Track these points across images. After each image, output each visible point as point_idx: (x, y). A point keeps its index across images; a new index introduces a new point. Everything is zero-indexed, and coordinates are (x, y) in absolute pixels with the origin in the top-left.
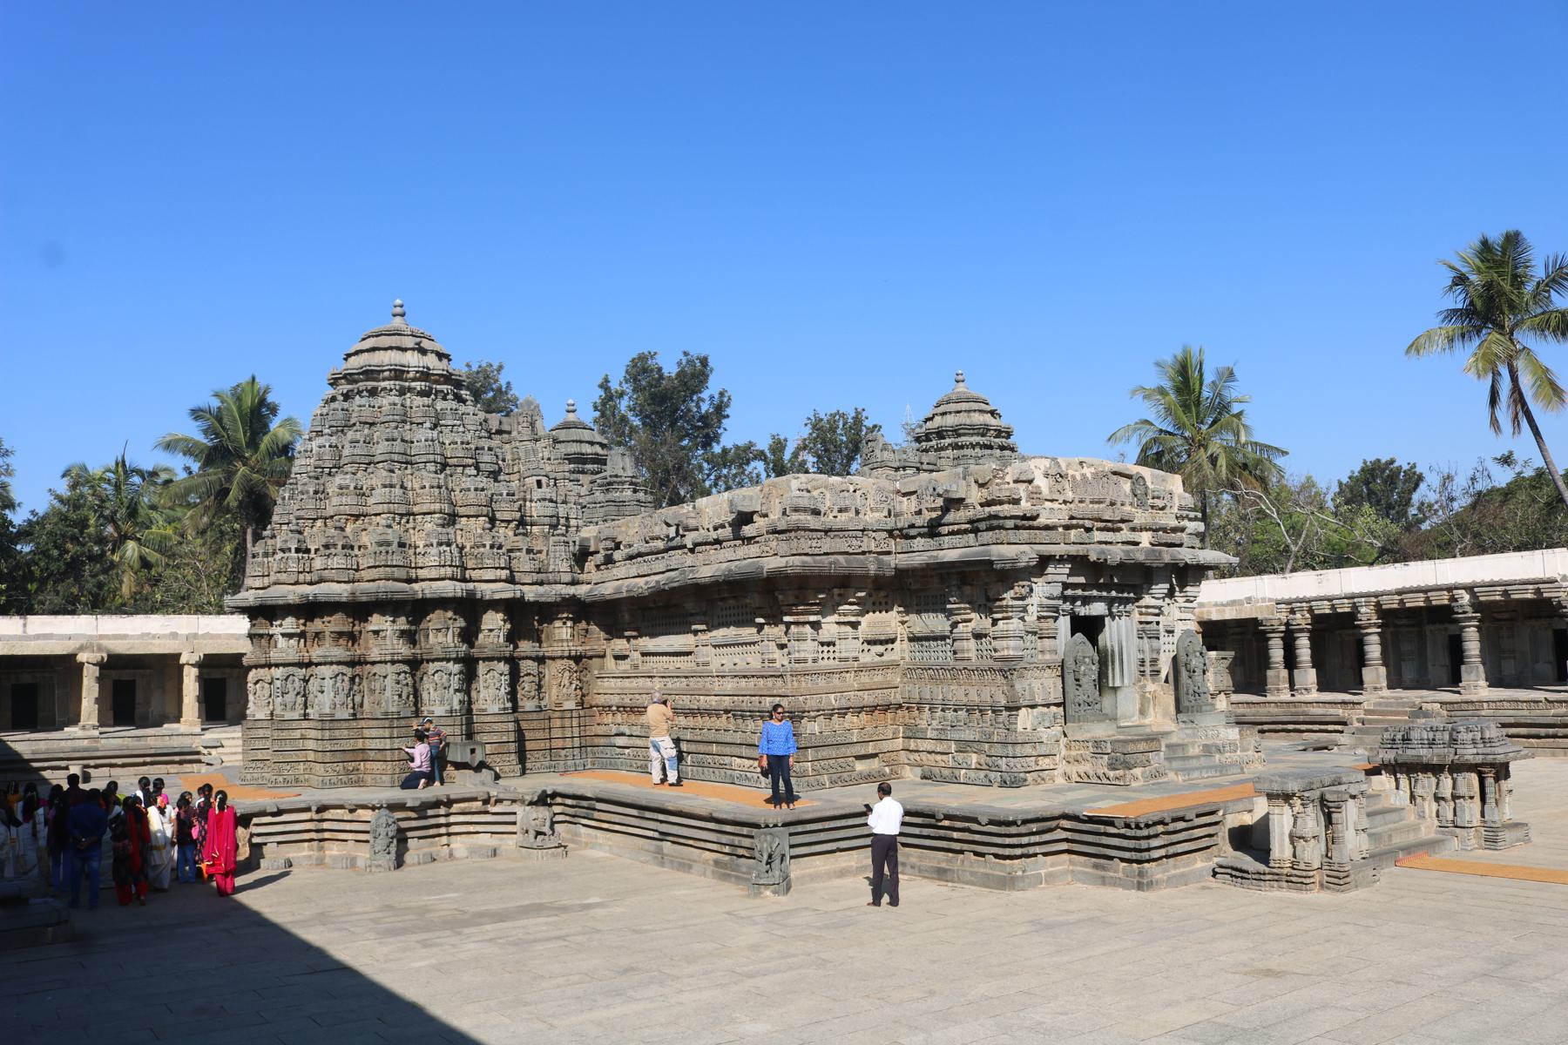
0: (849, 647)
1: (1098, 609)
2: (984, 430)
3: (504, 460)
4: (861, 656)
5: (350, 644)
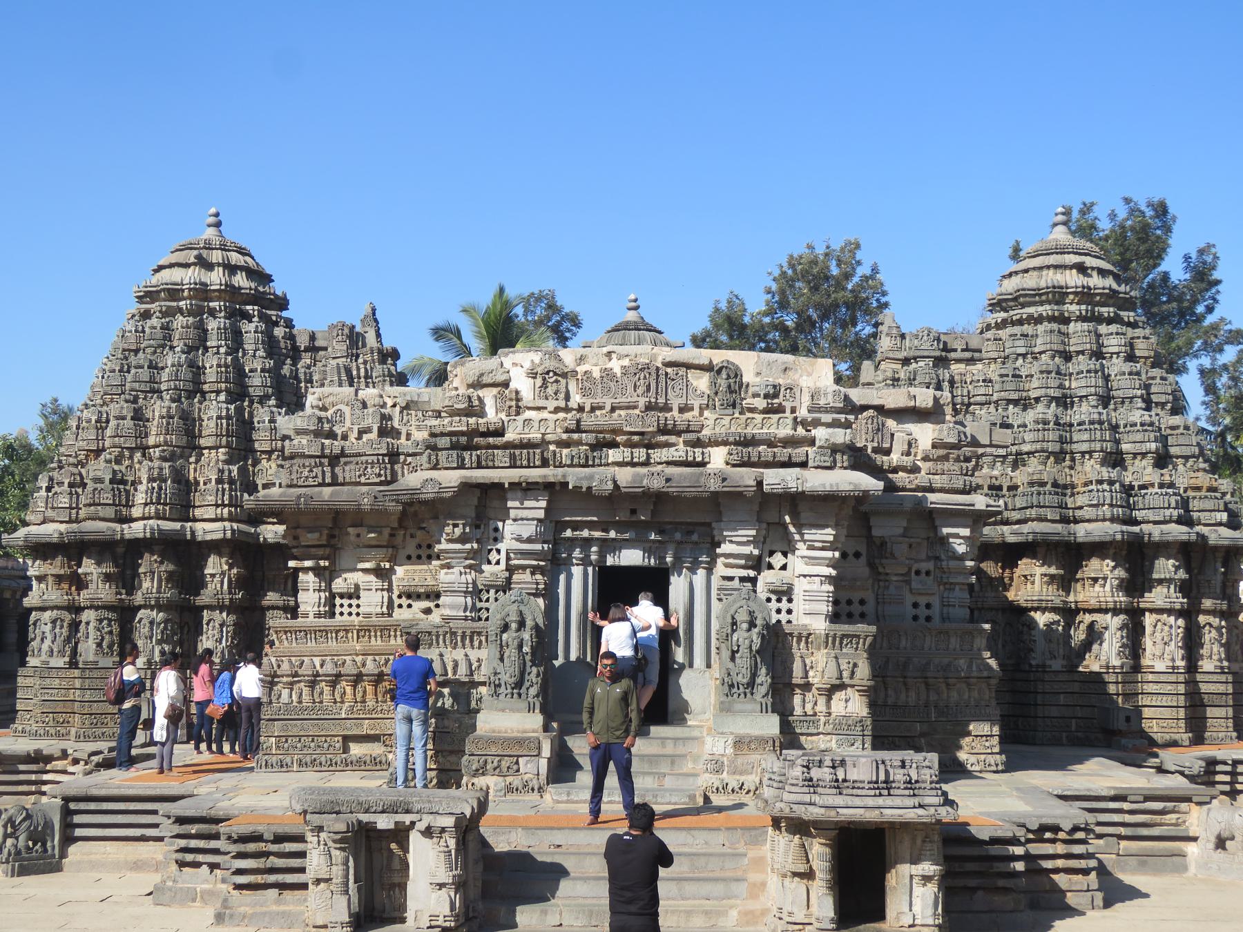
0: (372, 601)
1: (632, 557)
2: (1058, 295)
3: (311, 381)
4: (397, 614)
5: (73, 588)
